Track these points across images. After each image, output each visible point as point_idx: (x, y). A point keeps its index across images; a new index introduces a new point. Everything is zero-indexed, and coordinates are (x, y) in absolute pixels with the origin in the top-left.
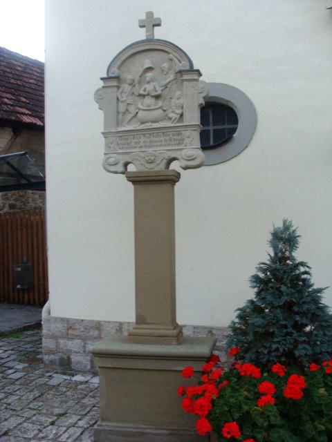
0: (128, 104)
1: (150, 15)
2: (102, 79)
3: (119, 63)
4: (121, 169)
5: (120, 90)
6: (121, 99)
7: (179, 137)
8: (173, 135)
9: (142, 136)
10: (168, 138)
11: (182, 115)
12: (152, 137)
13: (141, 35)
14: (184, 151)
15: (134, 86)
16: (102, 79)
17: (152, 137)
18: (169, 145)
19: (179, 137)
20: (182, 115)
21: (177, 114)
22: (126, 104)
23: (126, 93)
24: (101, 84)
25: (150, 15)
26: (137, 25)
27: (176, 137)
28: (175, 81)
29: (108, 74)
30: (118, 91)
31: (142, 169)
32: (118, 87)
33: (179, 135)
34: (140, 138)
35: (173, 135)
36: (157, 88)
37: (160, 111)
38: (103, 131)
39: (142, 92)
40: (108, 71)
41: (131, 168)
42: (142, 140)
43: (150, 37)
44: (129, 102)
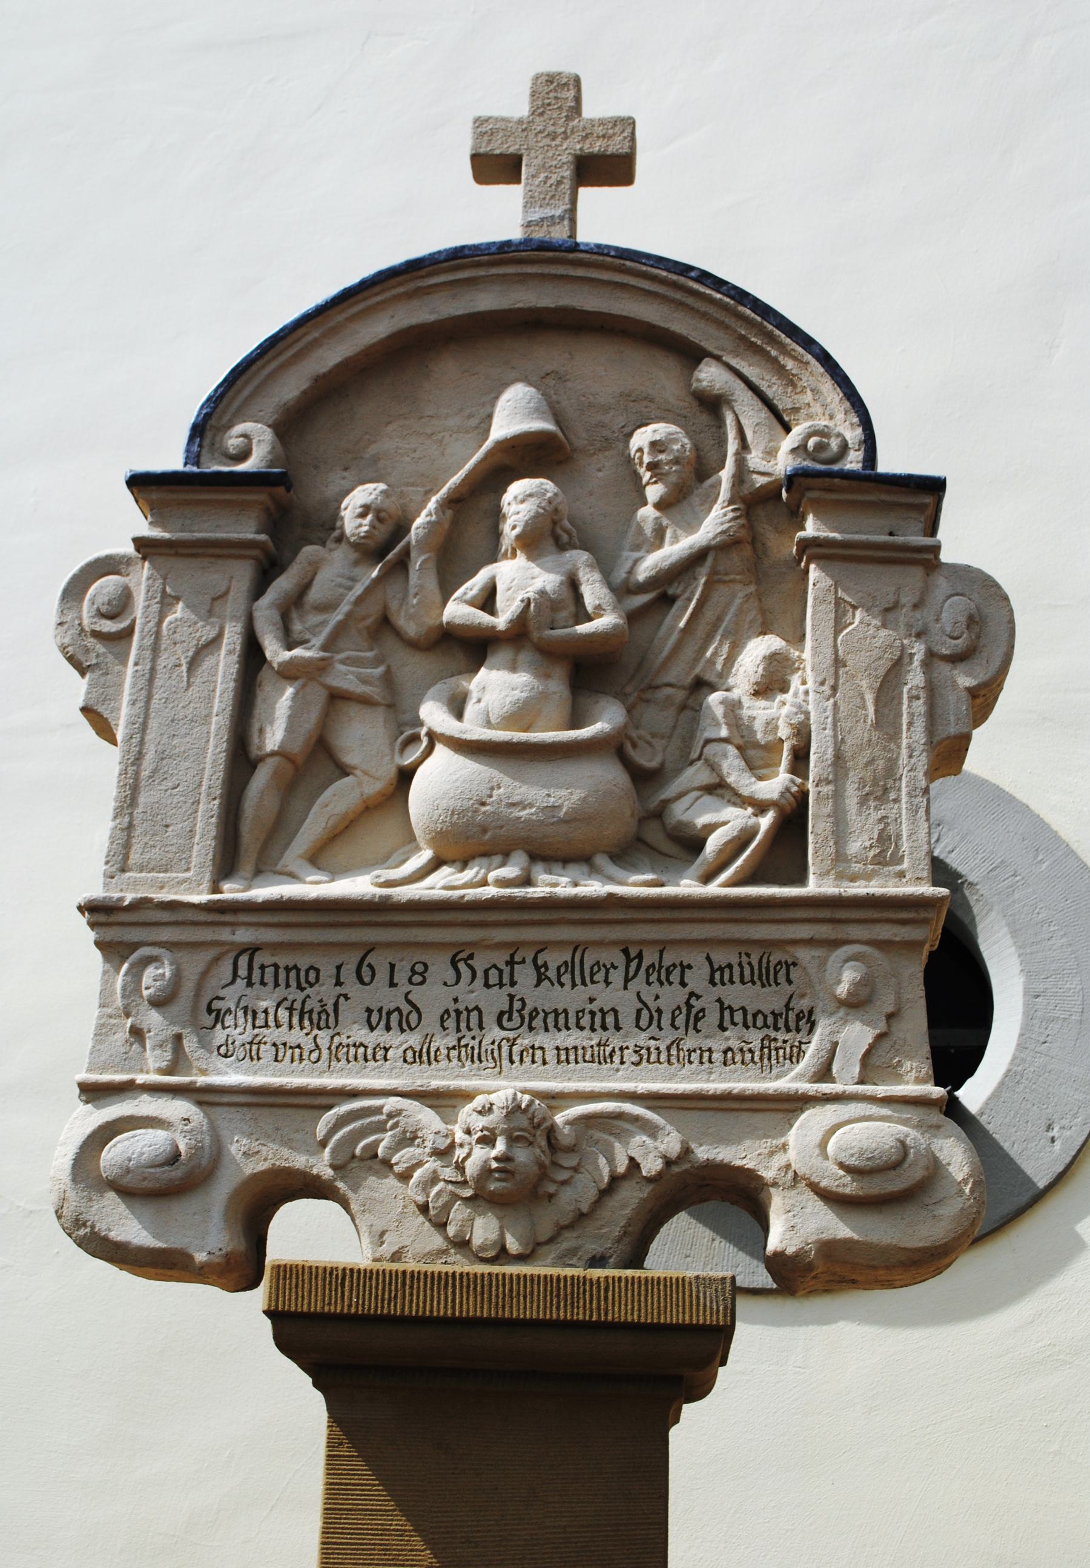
0: (336, 698)
1: (558, 93)
2: (139, 483)
3: (291, 387)
4: (209, 1236)
5: (283, 584)
6: (275, 652)
7: (769, 999)
8: (717, 974)
9: (440, 968)
10: (671, 996)
11: (793, 820)
12: (525, 975)
13: (499, 215)
14: (810, 1124)
15: (402, 564)
16: (139, 483)
17: (525, 975)
18: (675, 1055)
19: (769, 999)
20: (793, 820)
21: (761, 807)
22: (318, 697)
23: (327, 607)
24: (127, 523)
25: (558, 93)
26: (461, 148)
27: (737, 994)
28: (735, 560)
29: (193, 457)
30: (259, 590)
31: (419, 1246)
32: (267, 571)
33: (765, 977)
34: (419, 975)
35: (717, 974)
36: (593, 592)
37: (608, 775)
38: (97, 891)
39: (458, 610)
40: (204, 430)
41: (304, 1234)
42: (433, 997)
43: (559, 234)
44: (344, 677)
